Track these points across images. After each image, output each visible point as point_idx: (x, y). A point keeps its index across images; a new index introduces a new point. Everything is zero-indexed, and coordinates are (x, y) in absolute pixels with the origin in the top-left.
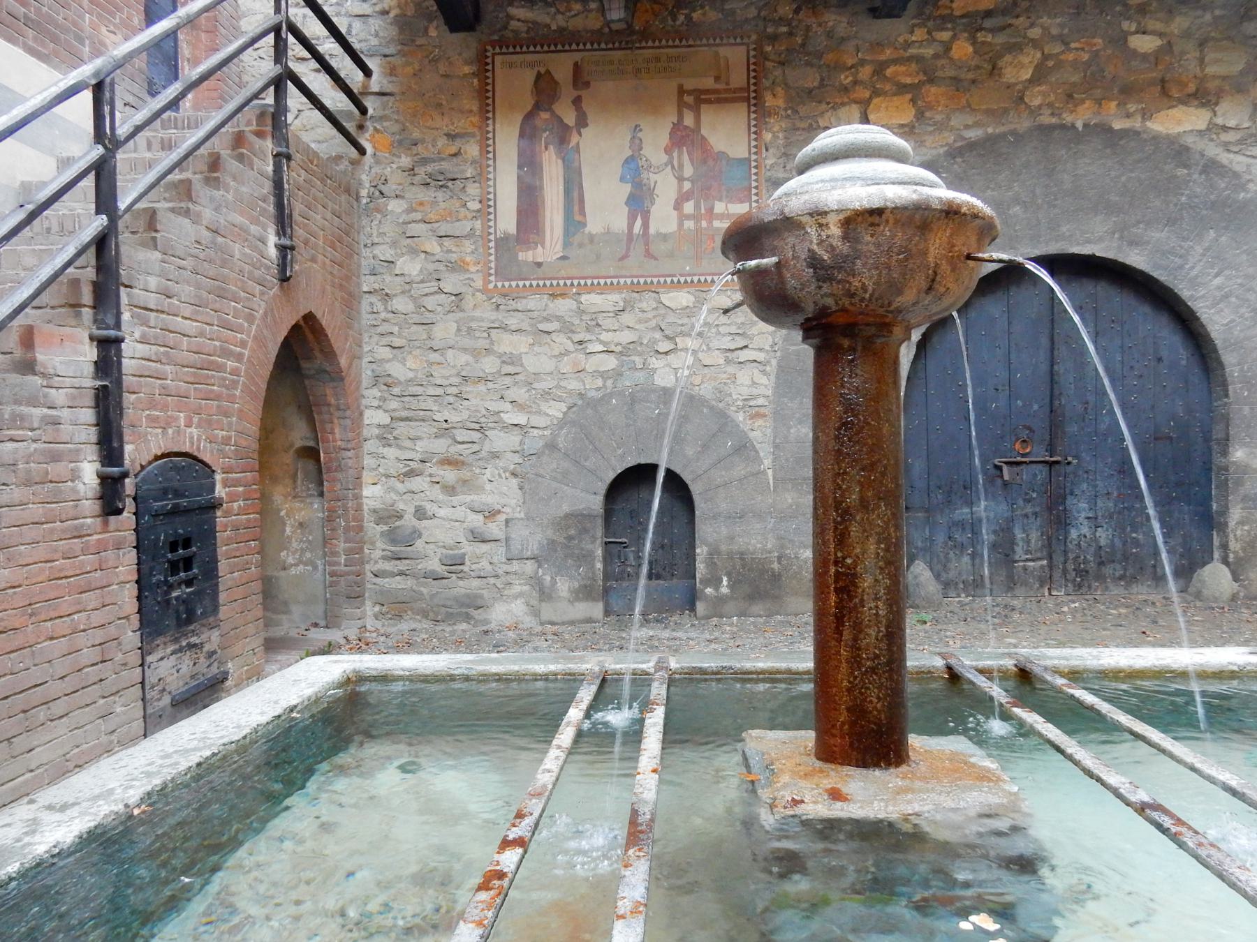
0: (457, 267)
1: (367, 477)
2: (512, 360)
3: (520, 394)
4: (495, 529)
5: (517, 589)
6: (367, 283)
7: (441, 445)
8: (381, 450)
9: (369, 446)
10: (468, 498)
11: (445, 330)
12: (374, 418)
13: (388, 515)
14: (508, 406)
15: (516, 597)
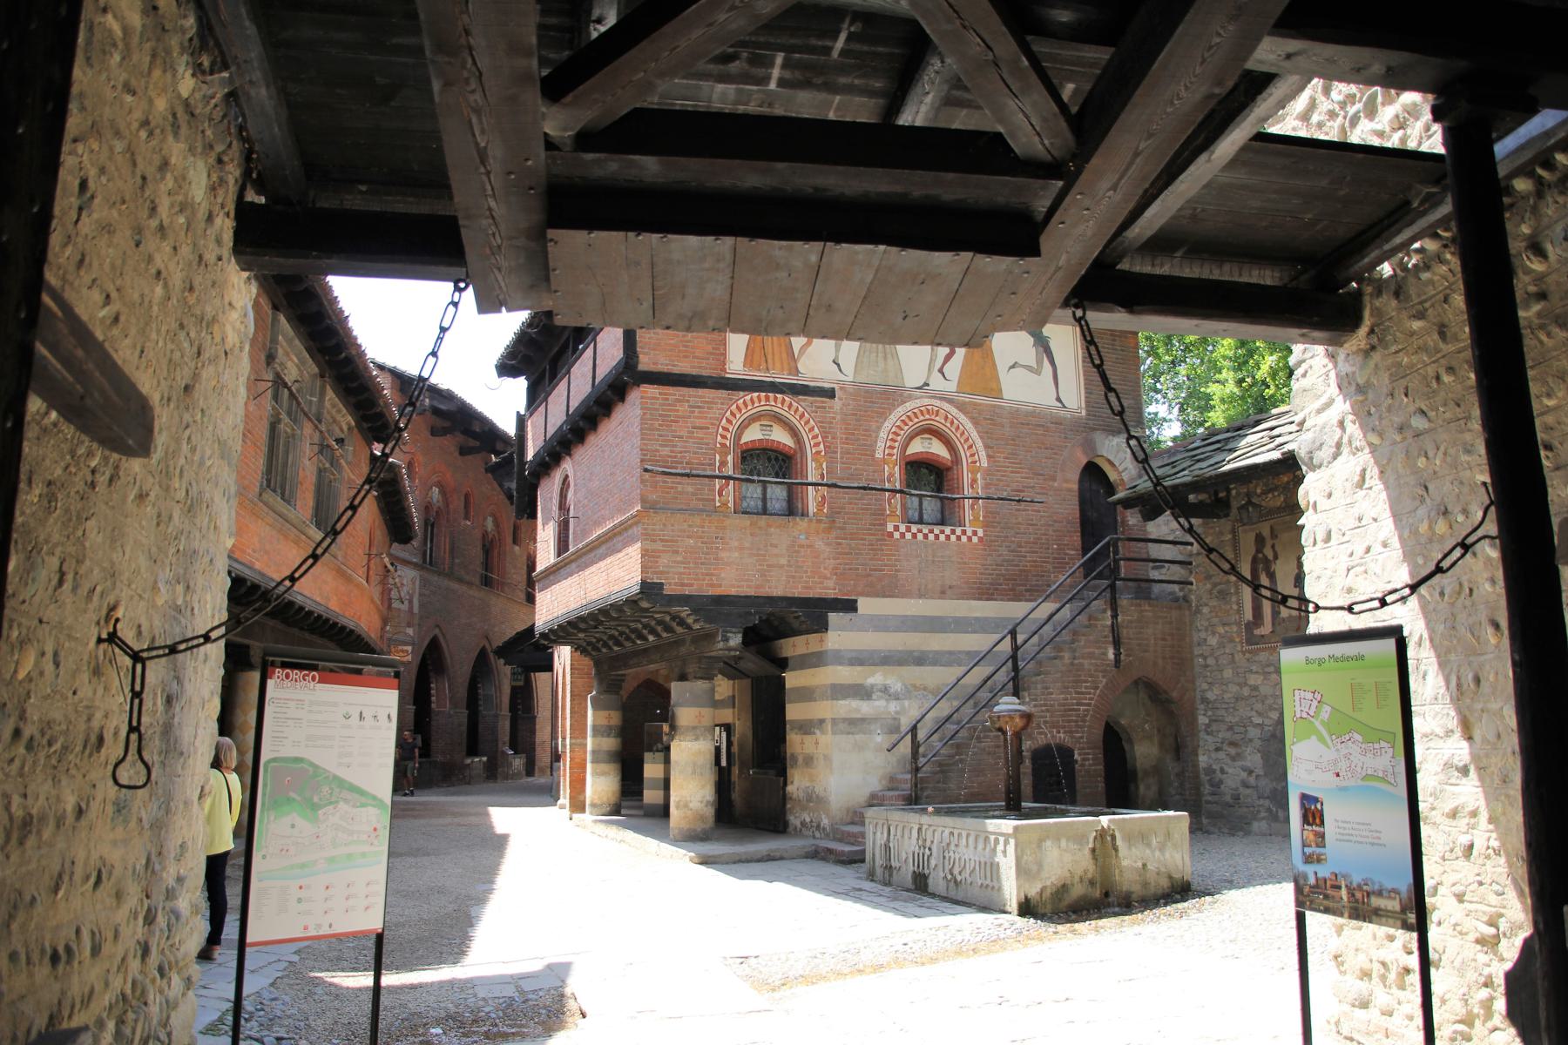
0: (1231, 640)
1: (1200, 751)
2: (1255, 688)
3: (1259, 706)
4: (1252, 780)
5: (1263, 814)
6: (1197, 651)
7: (1228, 735)
8: (1206, 737)
9: (1202, 735)
10: (1240, 763)
11: (1228, 673)
12: (1202, 720)
13: (1210, 771)
14: (1254, 713)
15: (1263, 818)
